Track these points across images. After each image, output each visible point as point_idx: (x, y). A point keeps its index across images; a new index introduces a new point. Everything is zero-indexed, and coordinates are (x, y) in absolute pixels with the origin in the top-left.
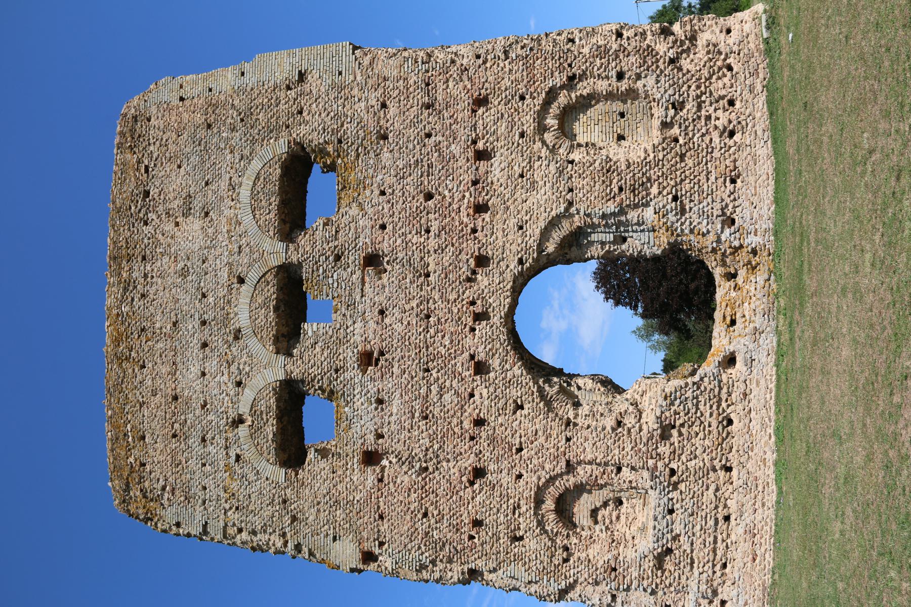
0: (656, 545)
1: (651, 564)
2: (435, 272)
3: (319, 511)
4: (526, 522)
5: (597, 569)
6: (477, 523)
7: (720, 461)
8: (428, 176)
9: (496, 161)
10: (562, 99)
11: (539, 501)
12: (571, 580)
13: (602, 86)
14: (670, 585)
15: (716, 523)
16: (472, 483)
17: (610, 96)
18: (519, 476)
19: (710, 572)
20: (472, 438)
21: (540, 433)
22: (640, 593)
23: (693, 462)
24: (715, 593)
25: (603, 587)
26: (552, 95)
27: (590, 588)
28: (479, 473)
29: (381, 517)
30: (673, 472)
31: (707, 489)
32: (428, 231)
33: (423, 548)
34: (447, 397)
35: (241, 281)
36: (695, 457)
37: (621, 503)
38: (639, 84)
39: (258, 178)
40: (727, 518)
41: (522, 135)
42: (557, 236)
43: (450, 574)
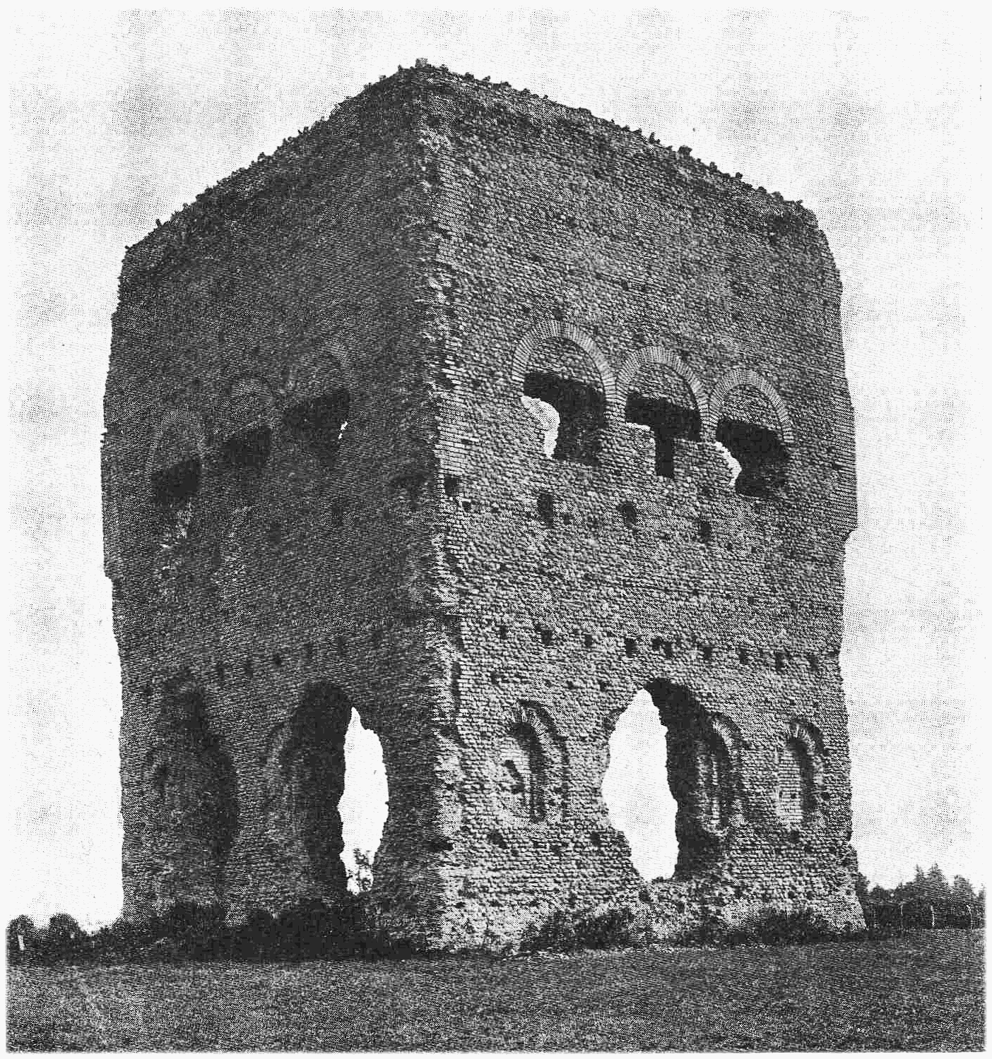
0: (507, 831)
1: (491, 827)
2: (698, 602)
3: (490, 424)
4: (516, 691)
5: (479, 768)
6: (503, 633)
7: (579, 893)
8: (765, 602)
10: (812, 744)
11: (524, 703)
12: (466, 741)
13: (818, 780)
14: (475, 848)
15: (531, 892)
16: (537, 628)
17: (809, 783)
18: (548, 684)
20: (575, 631)
21: (585, 709)
22: (458, 817)
23: (575, 867)
24: (473, 896)
25: (461, 776)
27: (457, 762)
28: (548, 638)
29: (494, 510)
30: (566, 845)
31: (556, 882)
32: (728, 597)
33: (471, 560)
34: (606, 605)
36: (579, 868)
37: (514, 792)
38: (819, 813)
40: (534, 904)
41: (792, 703)
42: (724, 733)
43: (446, 590)
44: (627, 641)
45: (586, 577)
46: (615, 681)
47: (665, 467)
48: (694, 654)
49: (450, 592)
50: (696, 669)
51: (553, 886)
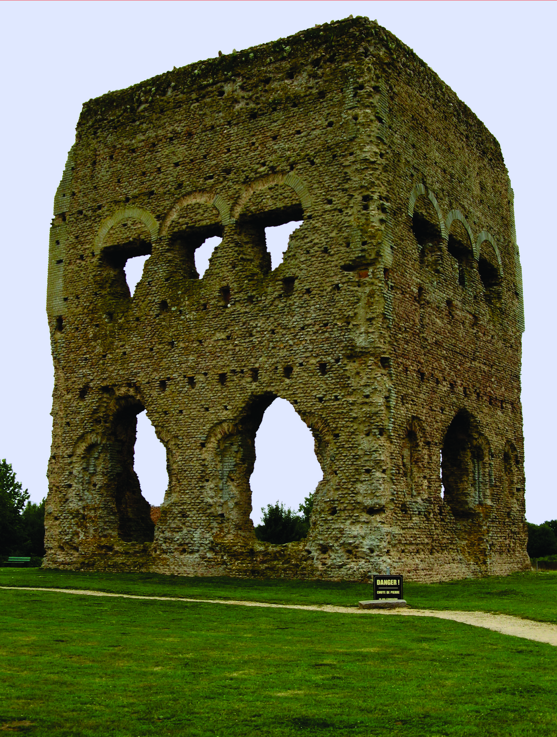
9: (500, 413)
15: (417, 544)
19: (403, 542)
26: (514, 449)
34: (443, 361)
35: (466, 217)
39: (494, 250)
44: (451, 384)
45: (436, 343)
46: (447, 409)
47: (462, 282)
48: (474, 396)
49: (385, 342)
50: (475, 405)
51: (426, 541)
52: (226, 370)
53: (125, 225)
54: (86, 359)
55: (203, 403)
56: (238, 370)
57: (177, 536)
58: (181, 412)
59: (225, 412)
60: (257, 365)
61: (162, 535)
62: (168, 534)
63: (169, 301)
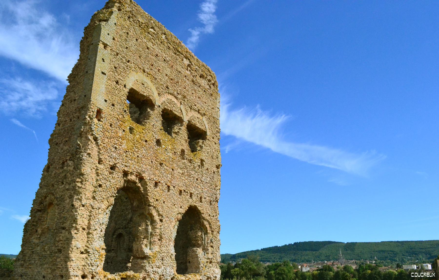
52: (182, 189)
53: (143, 84)
54: (116, 148)
55: (173, 201)
56: (186, 191)
57: (160, 271)
58: (164, 202)
59: (181, 209)
60: (192, 192)
61: (152, 270)
62: (155, 269)
63: (161, 141)
